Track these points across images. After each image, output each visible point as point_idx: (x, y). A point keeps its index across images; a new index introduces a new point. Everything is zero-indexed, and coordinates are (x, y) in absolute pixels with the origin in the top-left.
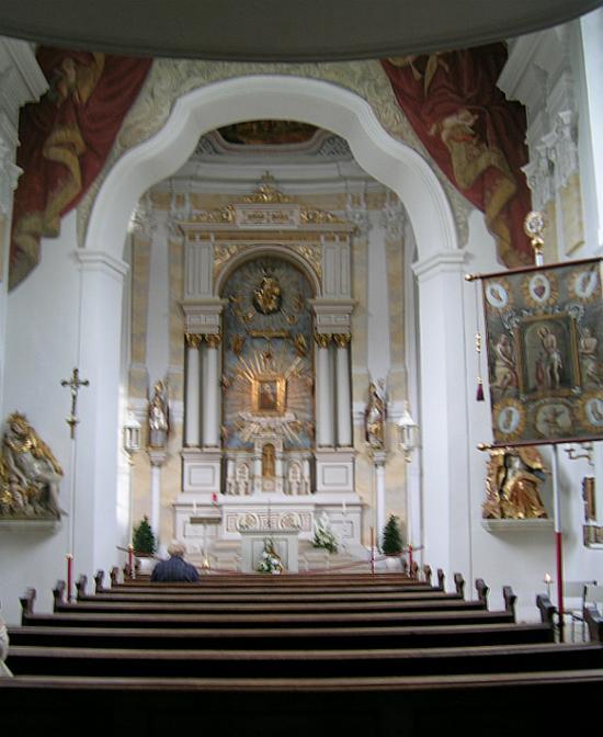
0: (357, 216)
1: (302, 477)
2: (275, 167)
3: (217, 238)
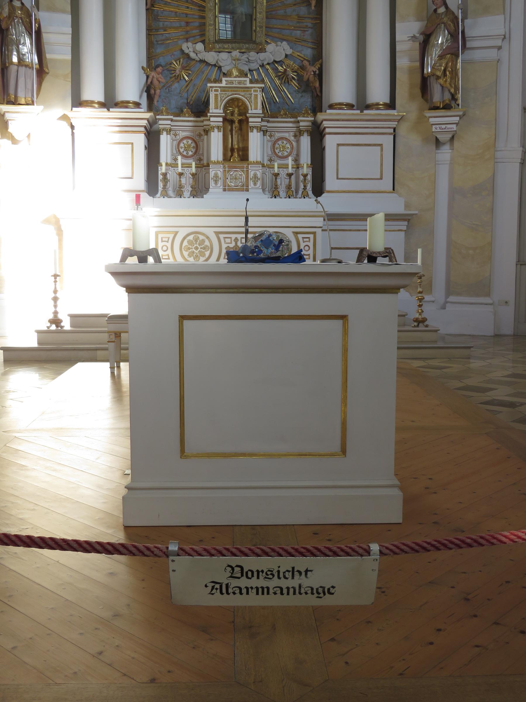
1: (297, 166)
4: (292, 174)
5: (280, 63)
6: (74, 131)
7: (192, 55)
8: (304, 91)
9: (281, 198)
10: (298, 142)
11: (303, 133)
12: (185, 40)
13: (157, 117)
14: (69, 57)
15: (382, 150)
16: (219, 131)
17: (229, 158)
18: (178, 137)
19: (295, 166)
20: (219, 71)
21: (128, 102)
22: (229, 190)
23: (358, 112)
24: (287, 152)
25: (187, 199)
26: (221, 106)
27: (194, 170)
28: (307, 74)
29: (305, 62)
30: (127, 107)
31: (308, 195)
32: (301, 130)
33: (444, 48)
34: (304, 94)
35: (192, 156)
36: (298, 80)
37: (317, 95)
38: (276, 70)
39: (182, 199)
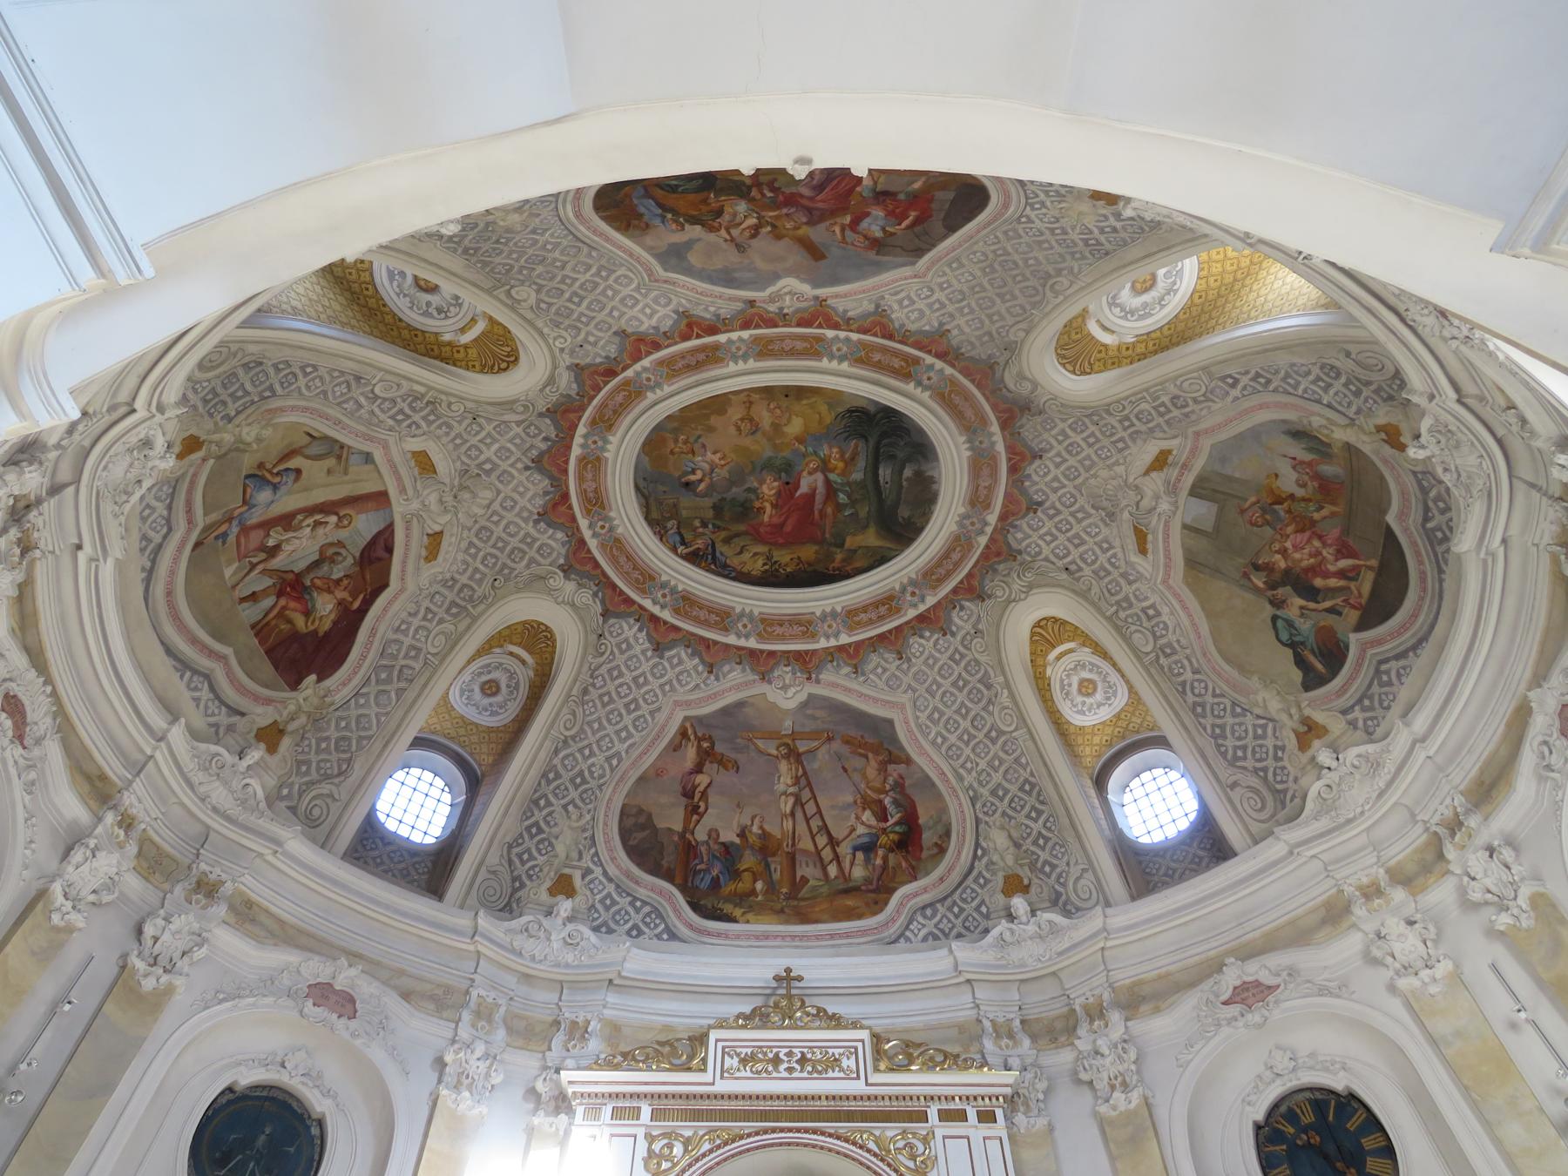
2: (804, 961)
3: (656, 1115)
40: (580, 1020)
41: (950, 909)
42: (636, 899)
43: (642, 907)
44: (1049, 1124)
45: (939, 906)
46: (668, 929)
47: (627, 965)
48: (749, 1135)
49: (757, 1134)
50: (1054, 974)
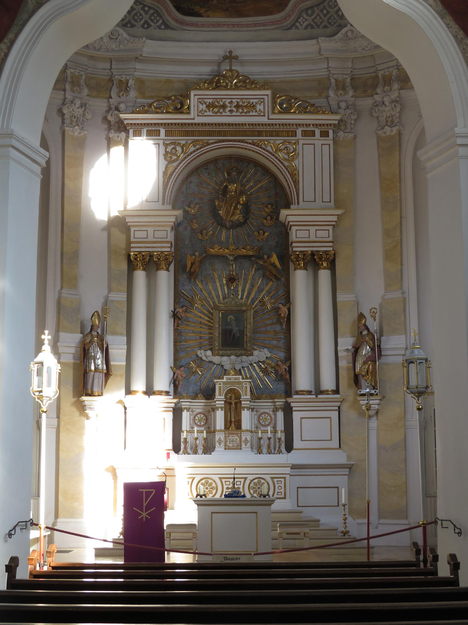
0: (343, 105)
1: (275, 431)
3: (168, 134)
4: (271, 438)
5: (263, 362)
6: (126, 411)
7: (204, 358)
8: (279, 380)
9: (264, 454)
10: (275, 415)
11: (279, 410)
12: (199, 348)
13: (181, 400)
14: (124, 363)
15: (331, 421)
16: (222, 410)
17: (229, 427)
18: (194, 413)
19: (273, 432)
20: (221, 368)
21: (162, 392)
22: (229, 449)
23: (314, 396)
24: (268, 422)
25: (200, 455)
26: (223, 393)
27: (205, 436)
28: (281, 370)
29: (279, 362)
30: (161, 395)
31: (281, 452)
32: (277, 408)
33: (367, 357)
34: (279, 382)
35: (203, 425)
36: (275, 373)
37: (288, 383)
38: (260, 367)
39: (197, 455)
40: (123, 79)
41: (322, 11)
42: (145, 6)
43: (149, 10)
44: (354, 136)
45: (316, 9)
46: (164, 23)
47: (144, 49)
48: (212, 143)
49: (216, 143)
50: (372, 56)
